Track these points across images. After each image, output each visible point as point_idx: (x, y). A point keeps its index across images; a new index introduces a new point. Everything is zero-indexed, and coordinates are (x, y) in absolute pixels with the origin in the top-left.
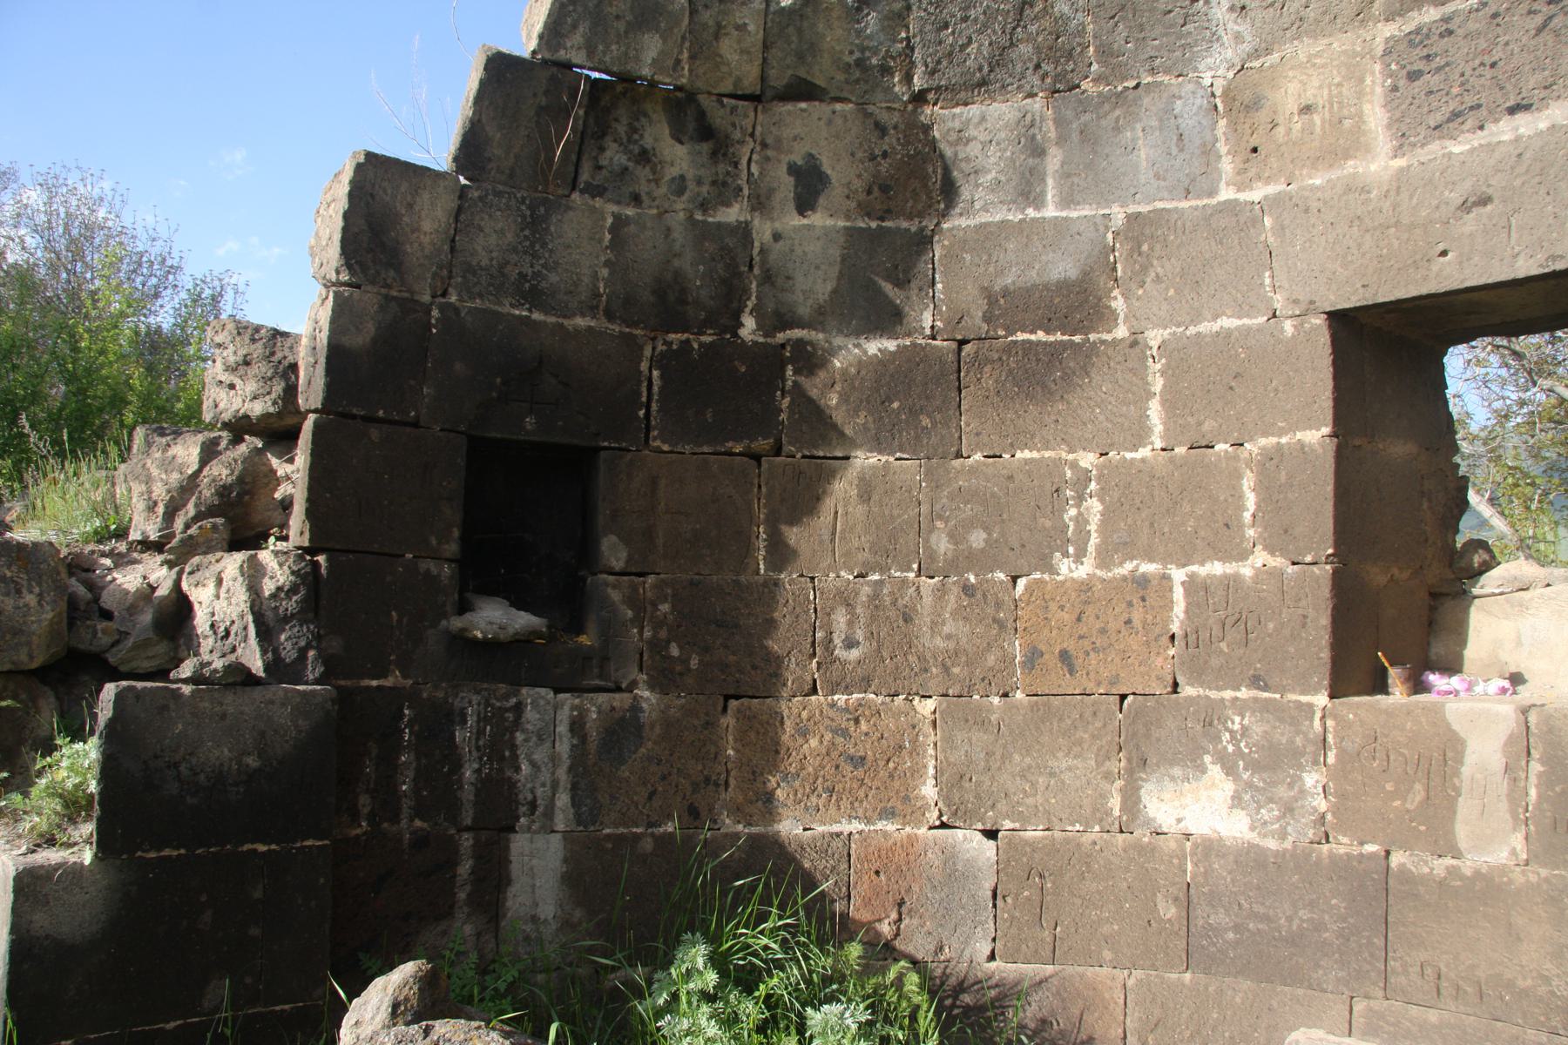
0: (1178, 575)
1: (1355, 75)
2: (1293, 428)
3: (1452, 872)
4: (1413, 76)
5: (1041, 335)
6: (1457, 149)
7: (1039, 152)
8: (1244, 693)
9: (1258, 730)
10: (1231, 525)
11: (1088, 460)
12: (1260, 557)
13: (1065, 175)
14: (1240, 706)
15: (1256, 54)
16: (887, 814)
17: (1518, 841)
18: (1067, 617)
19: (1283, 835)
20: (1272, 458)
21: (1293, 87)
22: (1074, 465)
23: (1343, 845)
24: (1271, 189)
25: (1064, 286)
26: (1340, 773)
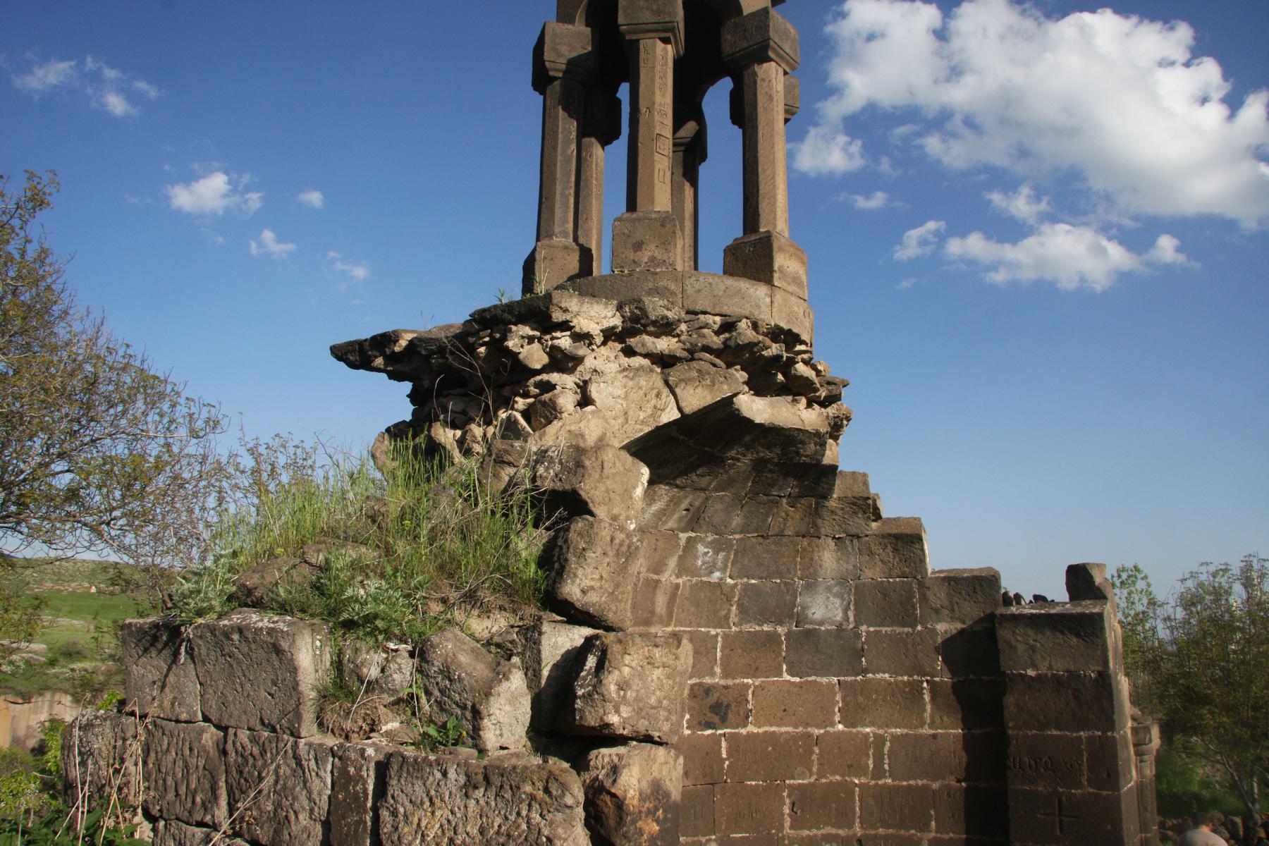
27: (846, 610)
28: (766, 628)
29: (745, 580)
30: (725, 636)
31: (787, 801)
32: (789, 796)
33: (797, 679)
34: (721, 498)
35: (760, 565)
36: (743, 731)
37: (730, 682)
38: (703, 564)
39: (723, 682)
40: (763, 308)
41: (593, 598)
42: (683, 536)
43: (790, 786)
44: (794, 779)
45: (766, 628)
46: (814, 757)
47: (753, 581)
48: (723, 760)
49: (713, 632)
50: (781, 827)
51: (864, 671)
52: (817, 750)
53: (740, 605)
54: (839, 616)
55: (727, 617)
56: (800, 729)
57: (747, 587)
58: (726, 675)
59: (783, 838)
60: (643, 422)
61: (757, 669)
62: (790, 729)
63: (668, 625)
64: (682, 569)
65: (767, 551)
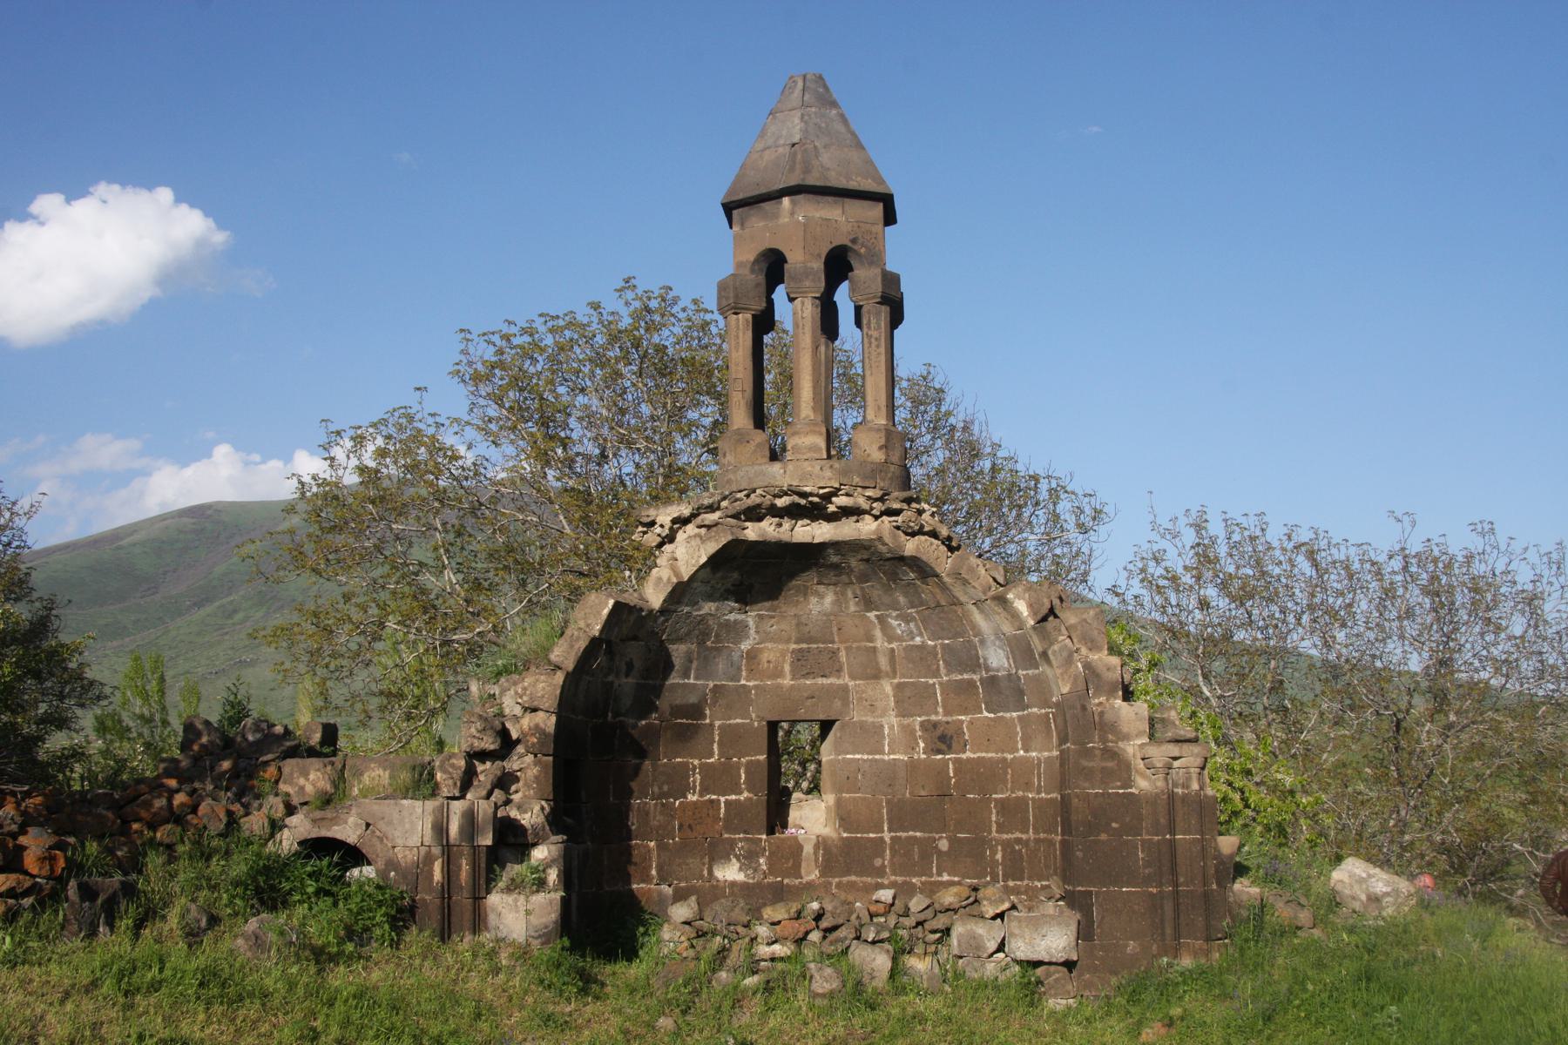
0: (722, 799)
1: (783, 655)
2: (756, 755)
3: (800, 883)
4: (799, 660)
5: (684, 721)
6: (808, 682)
7: (691, 662)
8: (741, 836)
9: (746, 847)
10: (738, 784)
11: (696, 762)
12: (746, 794)
13: (697, 670)
15: (758, 644)
17: (817, 872)
18: (690, 813)
19: (754, 878)
20: (749, 763)
21: (766, 655)
22: (692, 763)
23: (771, 879)
24: (756, 683)
25: (693, 705)
27: (1008, 658)
28: (966, 676)
29: (940, 641)
30: (940, 684)
31: (994, 811)
32: (995, 807)
33: (992, 715)
34: (873, 586)
35: (943, 629)
36: (964, 756)
37: (949, 719)
39: (945, 719)
40: (778, 478)
41: (557, 659)
42: (872, 615)
43: (995, 799)
44: (996, 793)
45: (966, 676)
46: (1009, 777)
47: (947, 642)
48: (951, 778)
49: (931, 681)
50: (990, 832)
51: (1028, 707)
52: (1010, 771)
54: (1006, 665)
55: (938, 669)
56: (999, 755)
57: (944, 647)
58: (946, 713)
59: (991, 840)
60: (694, 566)
62: (993, 755)
63: (894, 677)
64: (891, 637)
65: (941, 618)
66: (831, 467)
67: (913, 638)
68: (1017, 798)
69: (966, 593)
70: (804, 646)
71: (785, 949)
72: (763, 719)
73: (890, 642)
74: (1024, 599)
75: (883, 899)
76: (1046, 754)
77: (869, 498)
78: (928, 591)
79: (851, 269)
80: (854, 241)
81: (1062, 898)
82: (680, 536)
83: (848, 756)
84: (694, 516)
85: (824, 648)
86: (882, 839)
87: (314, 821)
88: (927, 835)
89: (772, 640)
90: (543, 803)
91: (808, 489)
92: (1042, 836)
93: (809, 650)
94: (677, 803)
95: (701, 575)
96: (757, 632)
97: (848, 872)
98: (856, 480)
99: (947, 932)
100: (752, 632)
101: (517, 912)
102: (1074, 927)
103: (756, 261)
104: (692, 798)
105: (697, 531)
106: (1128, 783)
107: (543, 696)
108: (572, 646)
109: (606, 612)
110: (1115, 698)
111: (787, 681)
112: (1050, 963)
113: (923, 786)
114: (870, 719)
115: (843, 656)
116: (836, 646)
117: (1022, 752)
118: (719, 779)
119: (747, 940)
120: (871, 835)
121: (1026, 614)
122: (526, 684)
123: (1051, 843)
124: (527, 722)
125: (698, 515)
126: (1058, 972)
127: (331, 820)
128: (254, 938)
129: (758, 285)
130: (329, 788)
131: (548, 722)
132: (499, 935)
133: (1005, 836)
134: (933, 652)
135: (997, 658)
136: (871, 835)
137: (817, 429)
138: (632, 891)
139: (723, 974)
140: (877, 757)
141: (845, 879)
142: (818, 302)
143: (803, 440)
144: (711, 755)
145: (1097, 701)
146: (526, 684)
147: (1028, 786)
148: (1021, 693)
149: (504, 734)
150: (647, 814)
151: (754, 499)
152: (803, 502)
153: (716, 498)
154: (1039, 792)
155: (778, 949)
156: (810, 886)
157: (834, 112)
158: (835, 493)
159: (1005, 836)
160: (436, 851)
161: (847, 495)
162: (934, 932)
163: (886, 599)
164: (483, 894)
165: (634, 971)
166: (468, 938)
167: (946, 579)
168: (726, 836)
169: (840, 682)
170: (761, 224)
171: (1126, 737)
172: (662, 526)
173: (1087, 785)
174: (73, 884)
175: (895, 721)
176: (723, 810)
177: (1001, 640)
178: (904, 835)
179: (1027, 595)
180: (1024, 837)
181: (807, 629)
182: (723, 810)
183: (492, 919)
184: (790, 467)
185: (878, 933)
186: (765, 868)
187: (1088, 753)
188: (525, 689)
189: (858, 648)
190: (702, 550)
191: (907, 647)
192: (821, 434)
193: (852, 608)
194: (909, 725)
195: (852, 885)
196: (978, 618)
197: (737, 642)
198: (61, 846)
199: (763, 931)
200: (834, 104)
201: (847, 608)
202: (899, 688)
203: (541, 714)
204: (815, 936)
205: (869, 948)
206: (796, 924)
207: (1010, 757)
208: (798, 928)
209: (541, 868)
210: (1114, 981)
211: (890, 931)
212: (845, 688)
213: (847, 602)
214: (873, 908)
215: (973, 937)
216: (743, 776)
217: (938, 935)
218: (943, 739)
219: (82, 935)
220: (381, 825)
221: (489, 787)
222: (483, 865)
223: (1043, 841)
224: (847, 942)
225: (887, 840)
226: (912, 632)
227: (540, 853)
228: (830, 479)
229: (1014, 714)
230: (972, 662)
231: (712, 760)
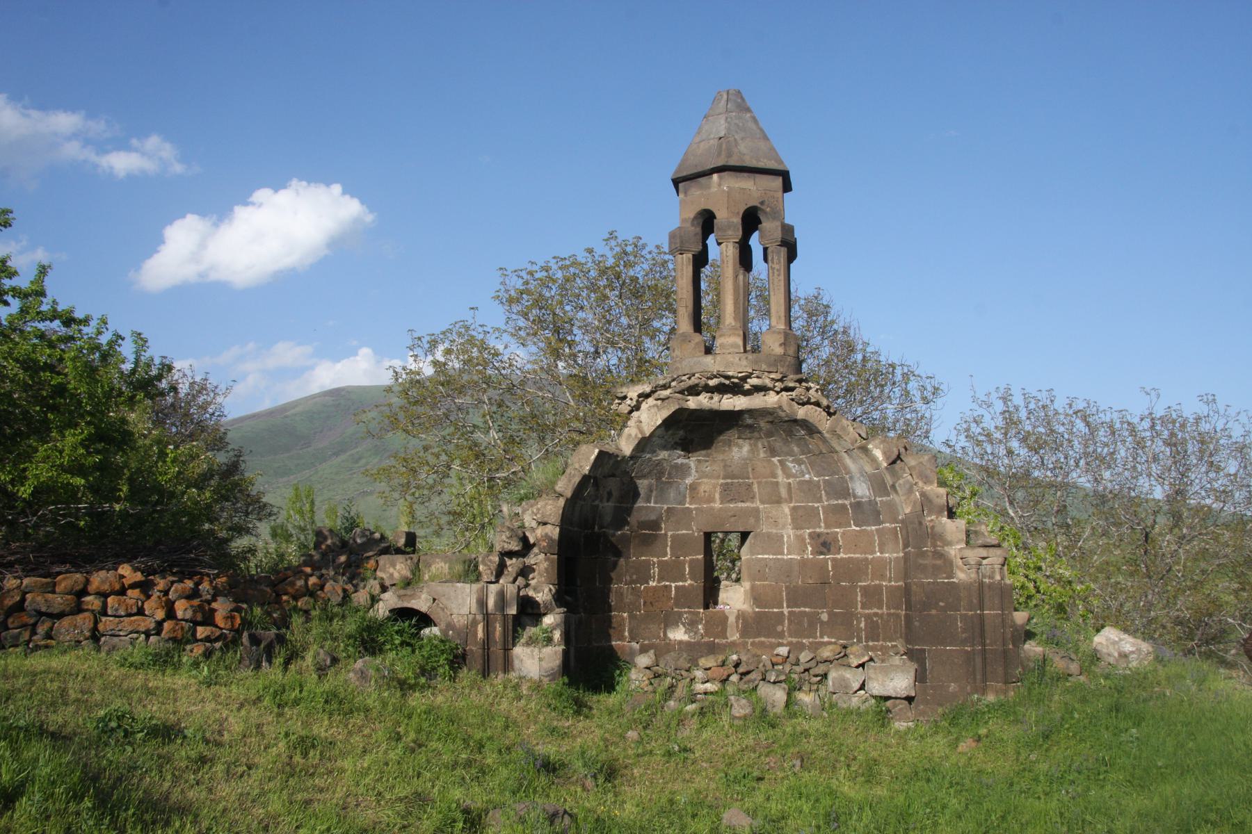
0: (673, 585)
1: (715, 487)
5: (647, 532)
6: (732, 506)
7: (651, 491)
8: (686, 610)
10: (684, 575)
11: (655, 560)
13: (656, 497)
14: (686, 613)
16: (620, 640)
17: (738, 635)
20: (691, 561)
23: (706, 639)
25: (653, 521)
26: (704, 625)
28: (840, 502)
30: (823, 507)
31: (859, 594)
33: (858, 529)
35: (824, 469)
36: (839, 556)
37: (829, 531)
38: (797, 471)
39: (826, 531)
42: (775, 460)
43: (860, 586)
44: (861, 582)
45: (840, 502)
46: (870, 571)
49: (816, 505)
50: (857, 609)
51: (882, 523)
52: (870, 567)
53: (825, 491)
54: (868, 494)
55: (821, 497)
57: (825, 481)
58: (827, 527)
61: (840, 524)
62: (859, 556)
64: (788, 475)
66: (747, 358)
67: (803, 476)
68: (875, 585)
69: (840, 444)
70: (729, 481)
71: (714, 686)
72: (701, 531)
73: (788, 478)
74: (880, 448)
75: (781, 653)
76: (895, 555)
77: (773, 379)
78: (813, 443)
79: (760, 223)
80: (762, 203)
81: (905, 654)
82: (644, 406)
83: (759, 556)
84: (653, 392)
85: (743, 483)
86: (782, 612)
87: (399, 597)
88: (813, 610)
89: (707, 476)
90: (551, 586)
91: (730, 374)
92: (892, 611)
93: (732, 484)
94: (643, 587)
95: (659, 432)
96: (697, 471)
97: (759, 635)
98: (764, 367)
99: (825, 676)
100: (693, 471)
101: (534, 659)
102: (912, 674)
103: (695, 218)
104: (652, 584)
105: (655, 402)
106: (951, 575)
107: (550, 515)
108: (570, 481)
109: (593, 457)
110: (942, 517)
111: (717, 505)
112: (896, 698)
113: (811, 577)
114: (774, 531)
115: (755, 487)
116: (751, 481)
117: (878, 554)
118: (672, 571)
119: (688, 680)
120: (775, 610)
121: (881, 459)
122: (539, 506)
123: (898, 616)
124: (540, 531)
125: (656, 391)
126: (902, 704)
127: (410, 596)
128: (360, 673)
129: (696, 235)
130: (409, 574)
131: (555, 532)
132: (522, 674)
133: (867, 611)
134: (817, 485)
135: (862, 490)
136: (775, 610)
137: (737, 332)
138: (611, 647)
139: (672, 703)
140: (779, 557)
141: (757, 640)
142: (737, 245)
143: (727, 339)
144: (665, 555)
145: (929, 519)
146: (539, 506)
147: (882, 577)
148: (878, 513)
149: (524, 539)
150: (622, 594)
151: (694, 381)
152: (727, 382)
153: (668, 380)
154: (890, 581)
155: (709, 686)
156: (733, 644)
157: (748, 115)
158: (749, 376)
159: (867, 611)
160: (479, 617)
161: (758, 377)
162: (816, 676)
163: (785, 449)
164: (510, 647)
165: (612, 700)
166: (501, 675)
167: (827, 435)
168: (676, 610)
169: (754, 505)
170: (698, 193)
171: (950, 544)
172: (631, 399)
173: (922, 576)
174: (245, 634)
175: (791, 532)
176: (673, 592)
177: (862, 475)
178: (797, 610)
179: (882, 446)
180: (880, 611)
181: (730, 469)
182: (673, 592)
183: (516, 663)
184: (718, 358)
185: (777, 676)
186: (702, 631)
187: (923, 555)
188: (538, 509)
189: (766, 482)
190: (658, 416)
191: (800, 481)
192: (739, 335)
193: (762, 455)
194: (801, 535)
195: (762, 644)
196: (848, 461)
197: (683, 478)
198: (238, 610)
199: (699, 674)
200: (748, 110)
201: (758, 455)
202: (794, 509)
203: (549, 526)
204: (734, 678)
205: (771, 686)
206: (721, 670)
207: (870, 557)
208: (723, 672)
209: (549, 630)
210: (940, 710)
211: (786, 675)
212: (757, 510)
213: (758, 451)
214: (774, 660)
215: (843, 679)
216: (687, 569)
217: (819, 678)
218: (825, 545)
219: (252, 667)
220: (443, 600)
221: (514, 575)
222: (510, 628)
223: (893, 614)
224: (756, 682)
225: (786, 613)
226: (803, 472)
227: (548, 620)
228: (746, 366)
229: (873, 528)
230: (845, 492)
231: (666, 558)
